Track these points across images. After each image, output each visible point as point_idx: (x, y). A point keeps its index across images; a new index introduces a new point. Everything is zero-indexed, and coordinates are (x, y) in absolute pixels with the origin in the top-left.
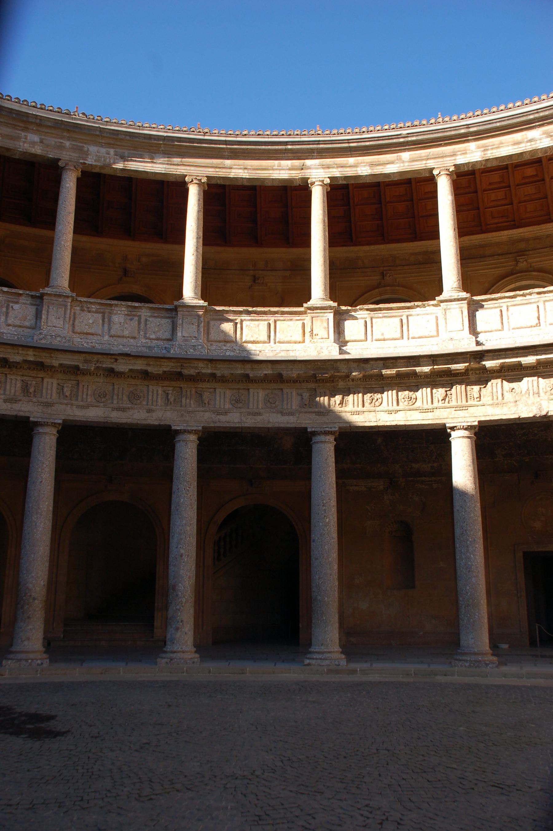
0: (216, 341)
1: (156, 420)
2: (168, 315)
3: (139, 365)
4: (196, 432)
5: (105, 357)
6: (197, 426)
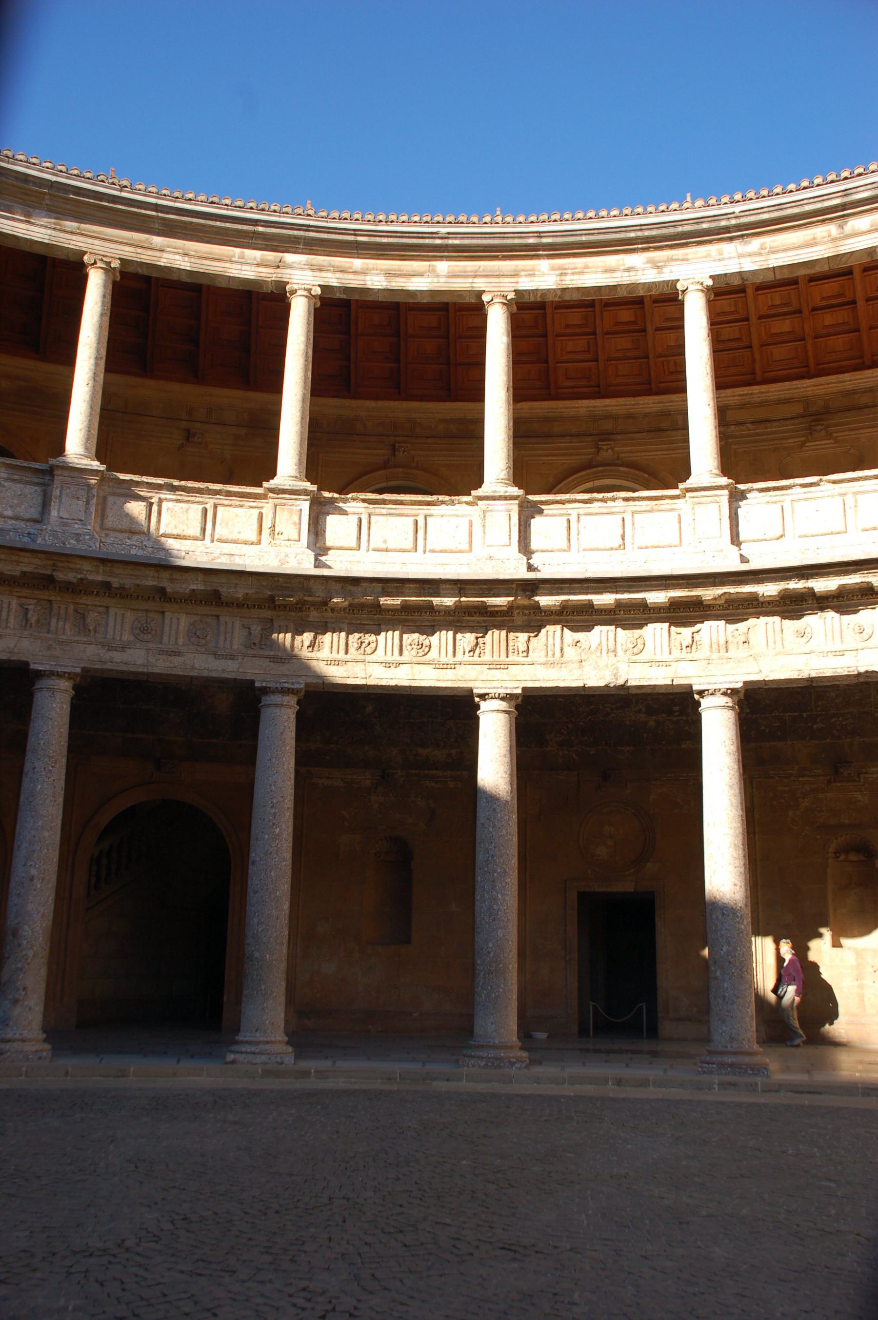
0: (115, 530)
2: (37, 480)
4: (70, 676)
6: (73, 667)
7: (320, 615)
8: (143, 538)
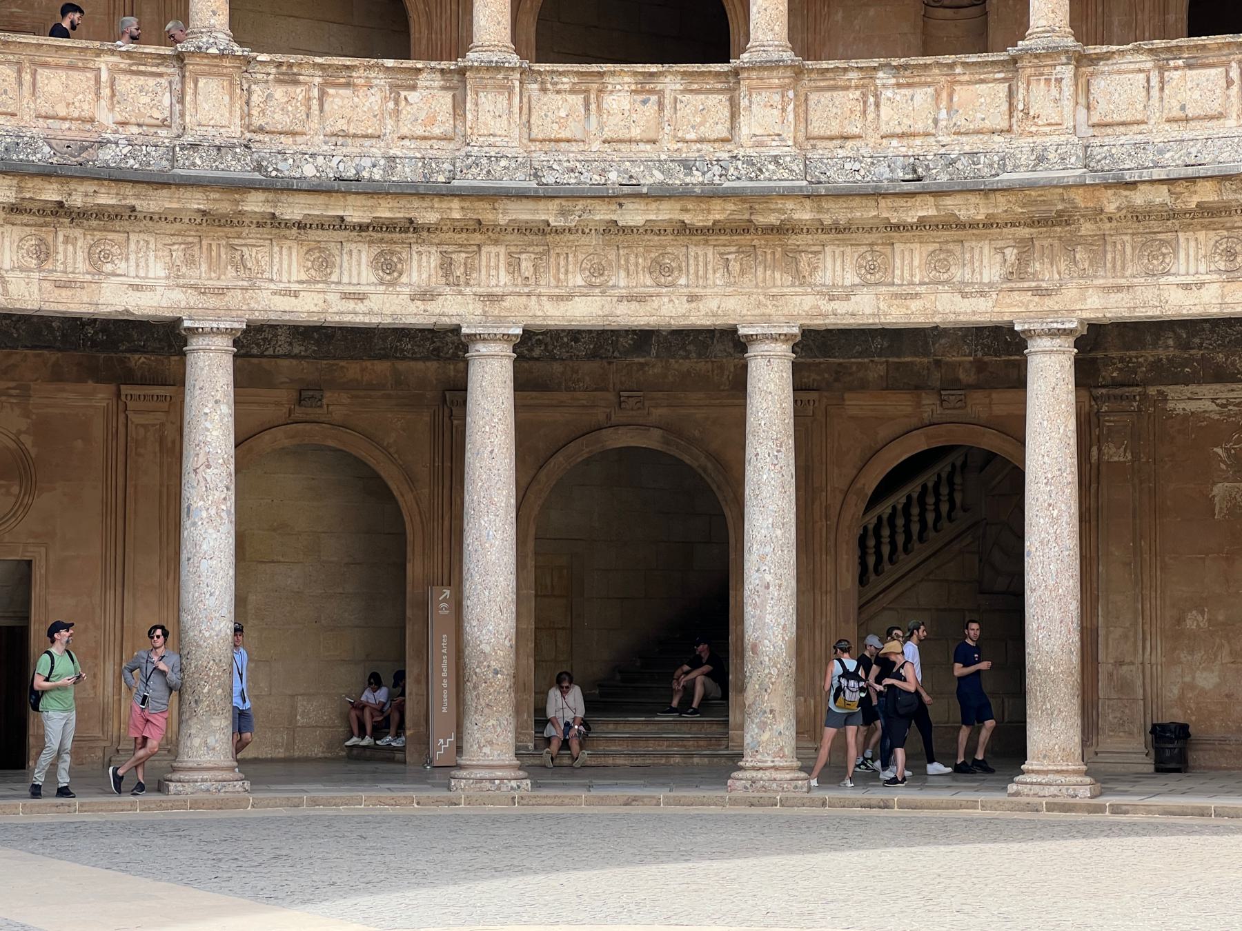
0: (822, 138)
1: (707, 314)
2: (720, 86)
3: (665, 213)
4: (787, 338)
5: (597, 201)
7: (1094, 227)
8: (858, 143)
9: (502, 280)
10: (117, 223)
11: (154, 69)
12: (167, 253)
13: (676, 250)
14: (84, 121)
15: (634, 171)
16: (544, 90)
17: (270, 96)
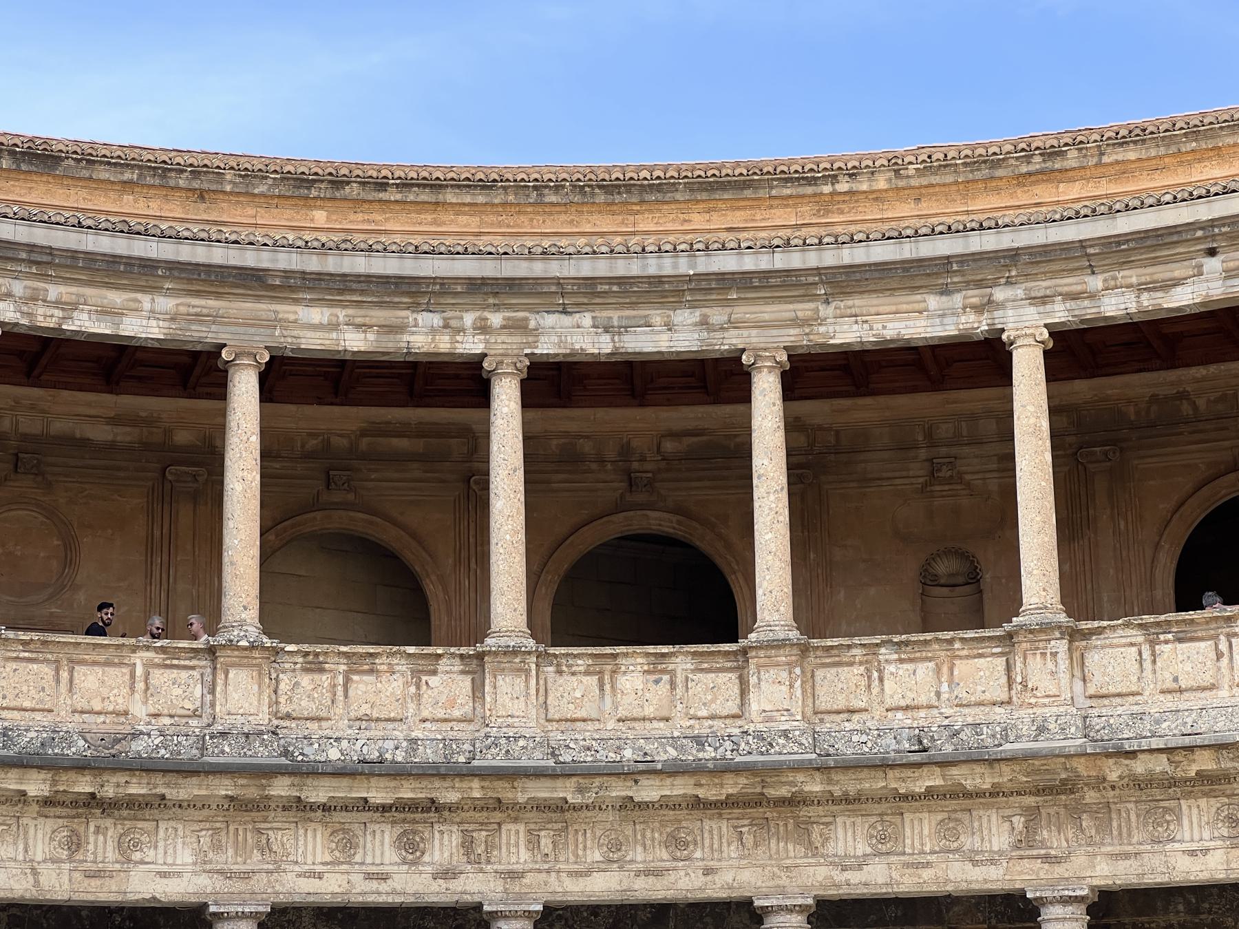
0: (829, 712)
1: (722, 887)
2: (729, 665)
3: (680, 788)
4: (802, 909)
5: (613, 778)
8: (864, 716)
9: (521, 857)
10: (147, 812)
11: (187, 663)
12: (194, 840)
13: (690, 823)
14: (118, 714)
15: (649, 747)
16: (560, 672)
17: (297, 684)
